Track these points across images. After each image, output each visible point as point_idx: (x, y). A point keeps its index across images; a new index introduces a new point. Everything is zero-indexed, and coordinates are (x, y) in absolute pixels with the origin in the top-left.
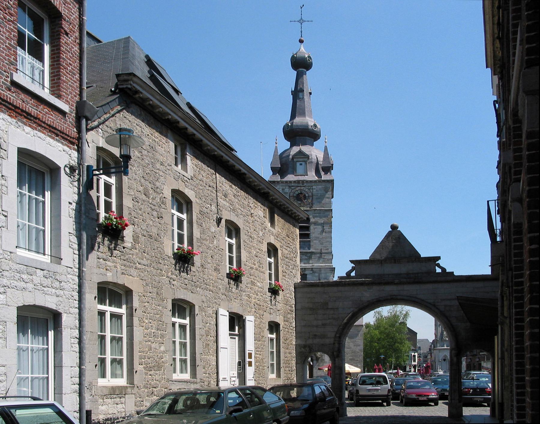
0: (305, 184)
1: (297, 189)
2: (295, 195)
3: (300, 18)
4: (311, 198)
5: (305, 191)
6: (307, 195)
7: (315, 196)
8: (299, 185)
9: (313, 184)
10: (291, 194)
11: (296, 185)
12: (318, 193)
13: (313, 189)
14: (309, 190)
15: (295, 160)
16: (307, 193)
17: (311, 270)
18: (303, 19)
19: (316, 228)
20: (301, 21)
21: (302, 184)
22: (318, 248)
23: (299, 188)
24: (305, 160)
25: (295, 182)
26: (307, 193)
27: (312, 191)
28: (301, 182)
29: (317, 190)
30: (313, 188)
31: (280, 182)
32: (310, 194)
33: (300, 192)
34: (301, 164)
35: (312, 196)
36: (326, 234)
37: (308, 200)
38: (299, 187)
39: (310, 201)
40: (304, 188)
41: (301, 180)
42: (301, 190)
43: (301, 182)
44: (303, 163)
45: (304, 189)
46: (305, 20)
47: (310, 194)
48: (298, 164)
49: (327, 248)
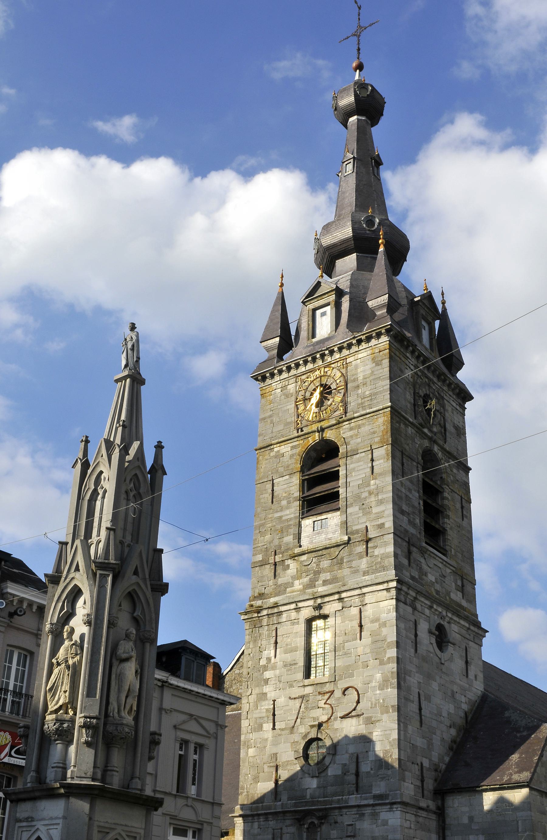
1: (313, 376)
6: (333, 386)
10: (300, 397)
17: (340, 599)
19: (354, 469)
22: (355, 528)
23: (317, 373)
27: (344, 371)
34: (323, 314)
36: (377, 482)
40: (326, 369)
44: (328, 309)
49: (381, 521)
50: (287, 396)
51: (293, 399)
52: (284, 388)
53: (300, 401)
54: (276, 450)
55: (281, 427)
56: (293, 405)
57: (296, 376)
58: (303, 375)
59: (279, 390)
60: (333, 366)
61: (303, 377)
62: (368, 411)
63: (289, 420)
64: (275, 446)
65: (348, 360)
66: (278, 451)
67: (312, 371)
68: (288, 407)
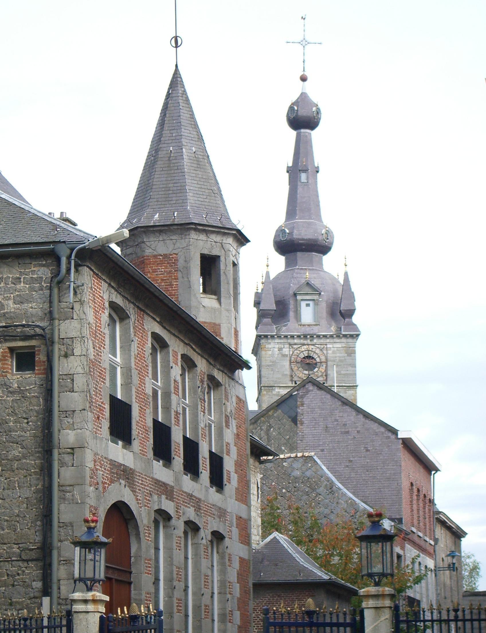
0: (315, 341)
2: (299, 360)
3: (302, 38)
4: (325, 365)
5: (315, 352)
6: (318, 360)
7: (331, 361)
8: (305, 342)
9: (328, 341)
11: (302, 341)
12: (336, 357)
13: (327, 350)
14: (321, 350)
15: (299, 297)
16: (319, 357)
18: (307, 39)
20: (304, 43)
21: (311, 340)
23: (305, 347)
24: (316, 297)
25: (299, 336)
26: (319, 357)
27: (325, 352)
28: (308, 337)
29: (334, 352)
30: (327, 348)
31: (276, 336)
32: (323, 359)
33: (306, 355)
34: (308, 305)
35: (326, 362)
37: (320, 369)
38: (306, 345)
39: (323, 371)
40: (313, 347)
41: (309, 335)
42: (308, 351)
43: (308, 337)
44: (311, 303)
45: (314, 350)
46: (309, 41)
47: (323, 359)
48: (303, 304)
50: (284, 356)
51: (288, 358)
52: (280, 349)
53: (293, 362)
54: (276, 390)
55: (280, 376)
56: (288, 363)
57: (290, 345)
58: (296, 345)
59: (276, 350)
60: (317, 346)
61: (295, 346)
62: (344, 385)
63: (285, 373)
64: (276, 388)
65: (329, 346)
66: (279, 392)
67: (304, 345)
68: (285, 364)
